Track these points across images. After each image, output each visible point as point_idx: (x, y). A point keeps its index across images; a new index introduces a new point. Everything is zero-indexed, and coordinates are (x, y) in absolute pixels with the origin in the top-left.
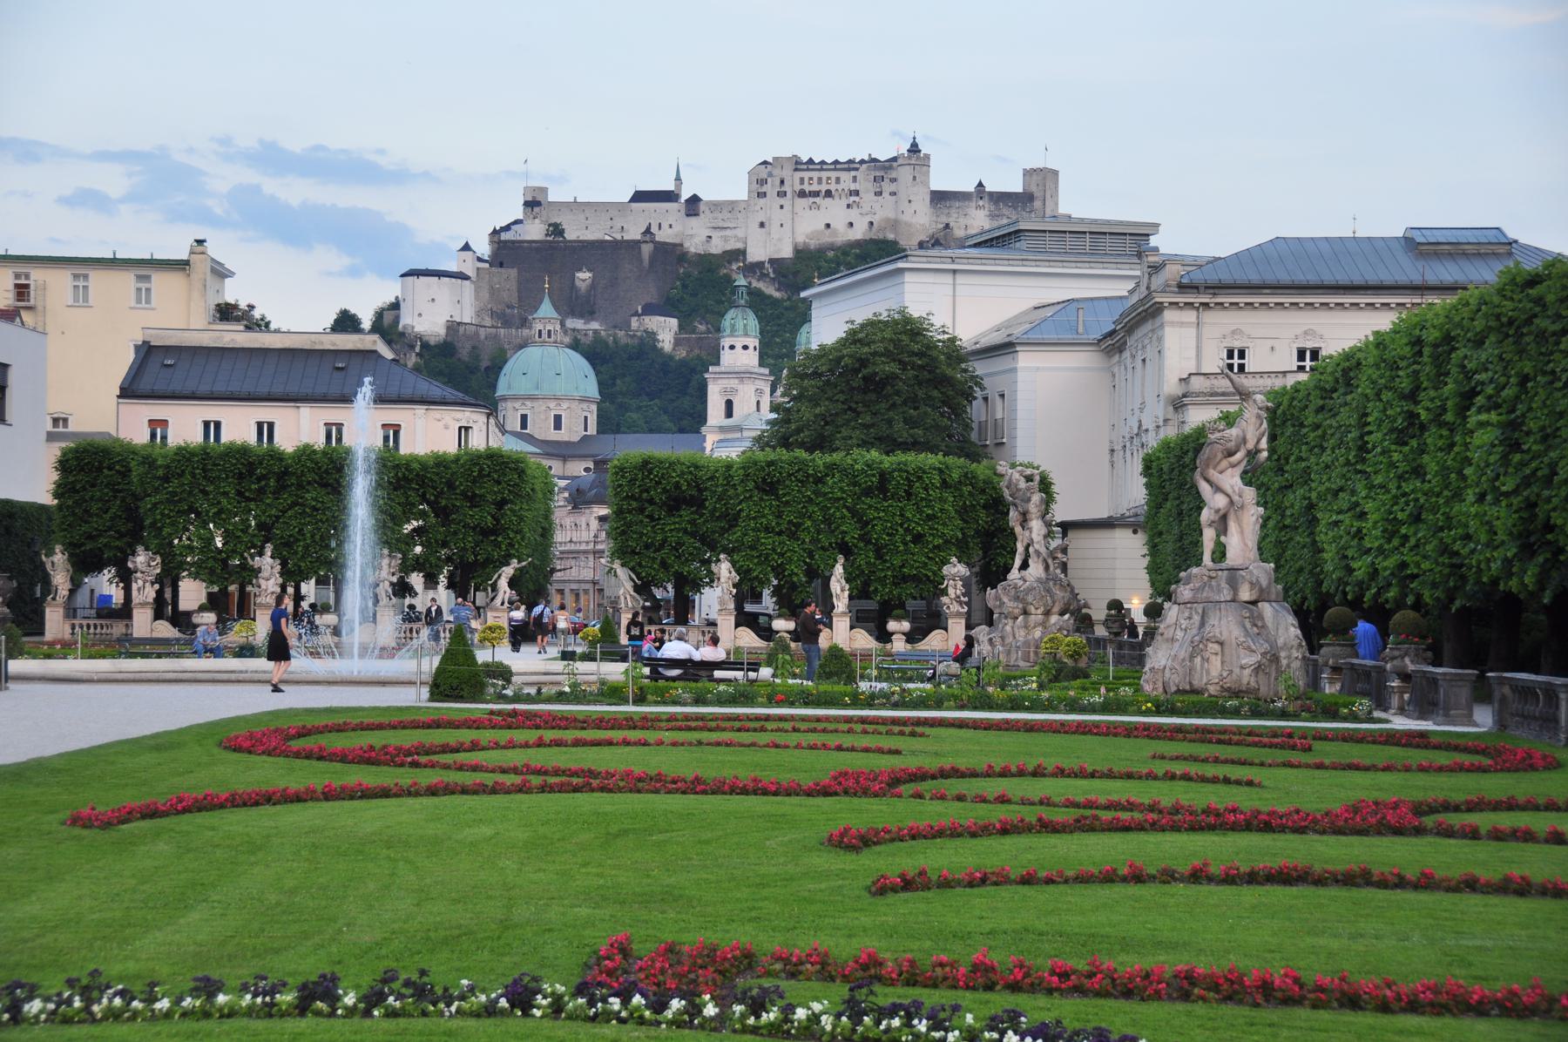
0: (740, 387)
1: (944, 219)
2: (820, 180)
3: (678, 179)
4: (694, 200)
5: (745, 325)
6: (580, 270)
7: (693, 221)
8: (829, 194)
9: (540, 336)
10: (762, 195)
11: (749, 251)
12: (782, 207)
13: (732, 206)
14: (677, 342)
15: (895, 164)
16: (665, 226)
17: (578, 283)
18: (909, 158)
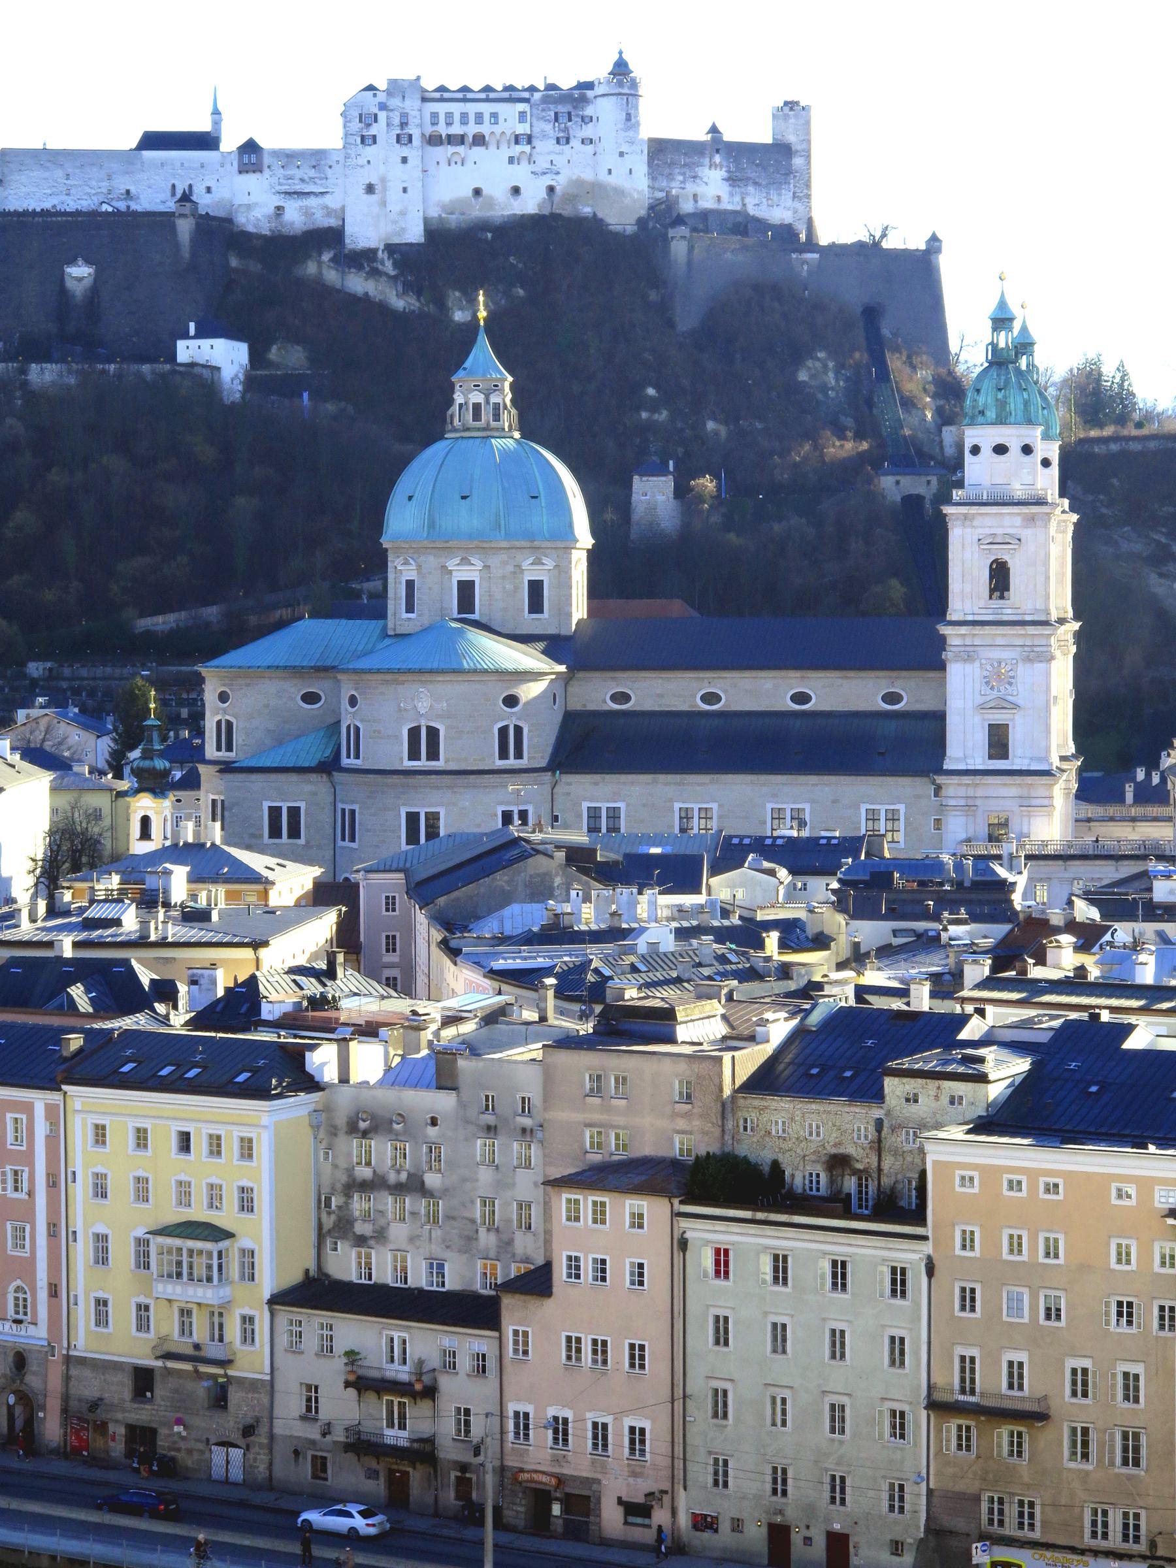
0: (1026, 533)
1: (664, 184)
2: (464, 119)
3: (216, 112)
4: (250, 147)
5: (1026, 403)
6: (72, 261)
7: (251, 181)
8: (479, 140)
9: (477, 415)
10: (368, 140)
11: (348, 230)
12: (404, 160)
13: (317, 158)
14: (251, 382)
17: (70, 284)
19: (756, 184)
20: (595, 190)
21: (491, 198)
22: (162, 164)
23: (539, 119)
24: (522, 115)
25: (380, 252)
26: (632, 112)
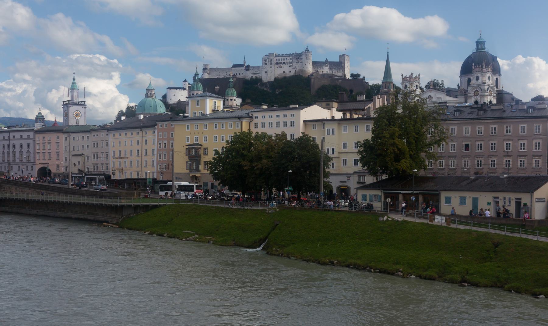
1: (316, 69)
3: (244, 61)
4: (248, 66)
5: (197, 87)
6: (216, 86)
8: (284, 63)
10: (266, 64)
11: (262, 79)
12: (271, 67)
13: (258, 67)
15: (302, 54)
16: (241, 74)
18: (305, 52)
19: (335, 69)
20: (302, 71)
21: (286, 73)
22: (235, 70)
23: (294, 59)
24: (291, 58)
25: (267, 83)
26: (308, 57)
